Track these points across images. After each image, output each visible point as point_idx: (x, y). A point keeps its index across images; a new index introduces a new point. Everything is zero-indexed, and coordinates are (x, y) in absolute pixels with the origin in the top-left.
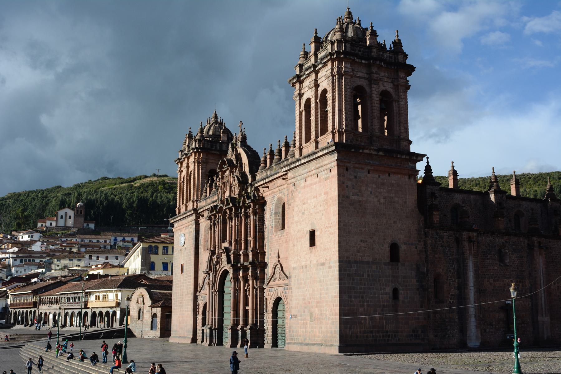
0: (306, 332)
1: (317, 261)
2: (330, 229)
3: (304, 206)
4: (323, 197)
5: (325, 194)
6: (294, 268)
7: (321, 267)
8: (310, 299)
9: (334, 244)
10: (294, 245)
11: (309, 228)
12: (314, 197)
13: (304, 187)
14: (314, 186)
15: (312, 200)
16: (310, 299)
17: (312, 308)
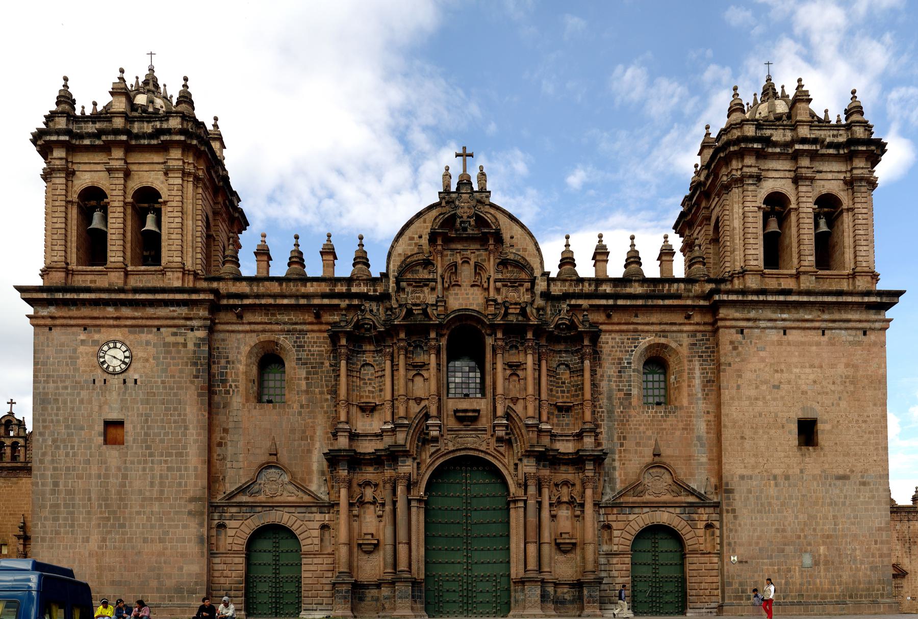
0: (787, 583)
1: (824, 471)
2: (863, 425)
3: (777, 376)
4: (841, 369)
5: (847, 366)
6: (742, 477)
7: (839, 483)
8: (802, 530)
9: (877, 449)
10: (742, 438)
11: (798, 413)
12: (812, 366)
13: (780, 343)
14: (814, 348)
15: (808, 370)
16: (802, 530)
17: (809, 544)
